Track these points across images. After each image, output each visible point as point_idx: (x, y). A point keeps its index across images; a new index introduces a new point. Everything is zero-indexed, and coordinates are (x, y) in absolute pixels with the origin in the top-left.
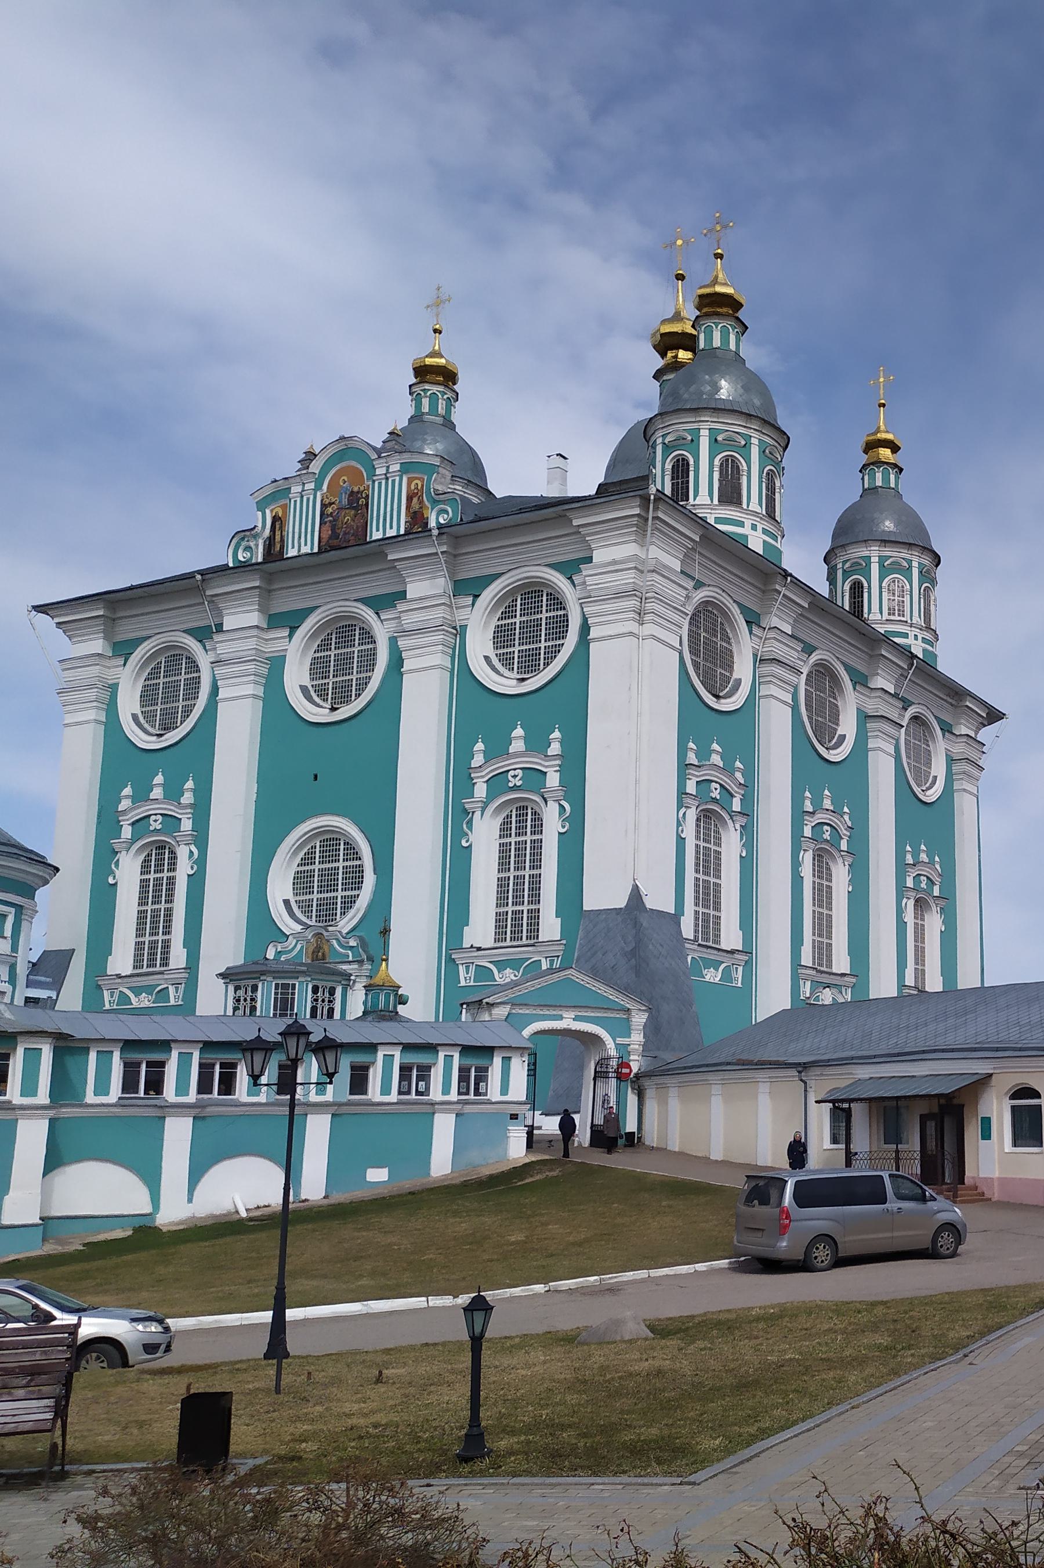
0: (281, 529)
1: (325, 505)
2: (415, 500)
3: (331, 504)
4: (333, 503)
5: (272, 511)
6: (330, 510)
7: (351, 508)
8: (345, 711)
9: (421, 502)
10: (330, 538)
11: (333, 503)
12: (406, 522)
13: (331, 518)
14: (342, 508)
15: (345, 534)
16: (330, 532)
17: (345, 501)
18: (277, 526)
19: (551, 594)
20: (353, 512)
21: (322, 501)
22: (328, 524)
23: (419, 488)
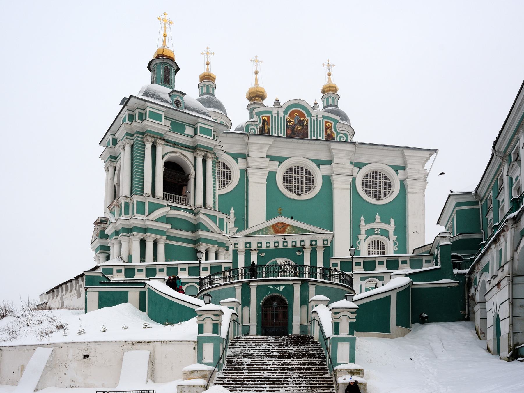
0: (268, 124)
1: (288, 121)
2: (328, 130)
3: (291, 122)
4: (292, 122)
5: (262, 117)
6: (291, 124)
7: (300, 125)
8: (305, 196)
9: (331, 131)
10: (291, 134)
11: (292, 122)
12: (325, 137)
13: (291, 127)
14: (296, 124)
15: (298, 134)
16: (291, 132)
17: (297, 122)
18: (266, 124)
19: (384, 175)
20: (301, 127)
21: (287, 120)
22: (290, 128)
23: (330, 126)
